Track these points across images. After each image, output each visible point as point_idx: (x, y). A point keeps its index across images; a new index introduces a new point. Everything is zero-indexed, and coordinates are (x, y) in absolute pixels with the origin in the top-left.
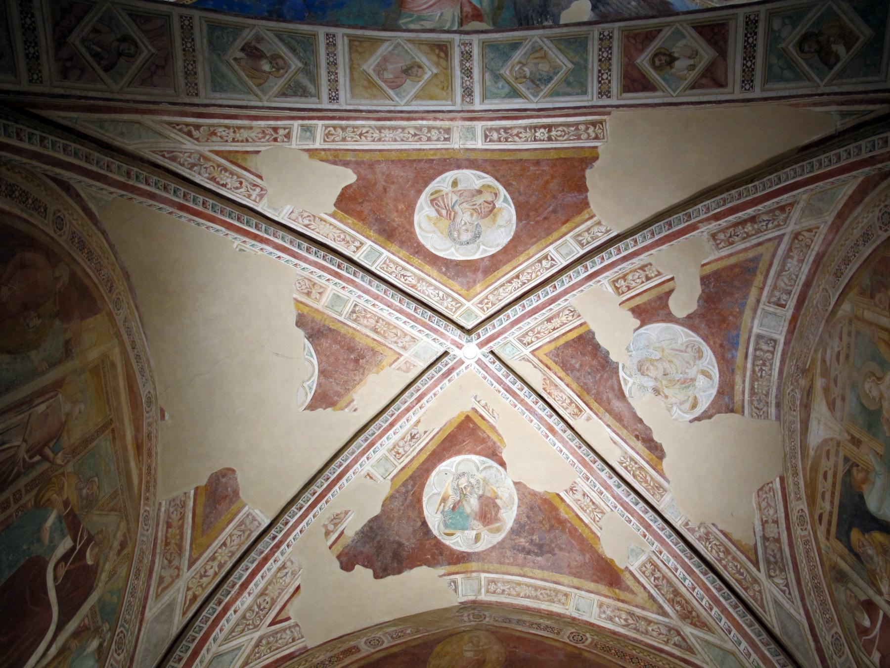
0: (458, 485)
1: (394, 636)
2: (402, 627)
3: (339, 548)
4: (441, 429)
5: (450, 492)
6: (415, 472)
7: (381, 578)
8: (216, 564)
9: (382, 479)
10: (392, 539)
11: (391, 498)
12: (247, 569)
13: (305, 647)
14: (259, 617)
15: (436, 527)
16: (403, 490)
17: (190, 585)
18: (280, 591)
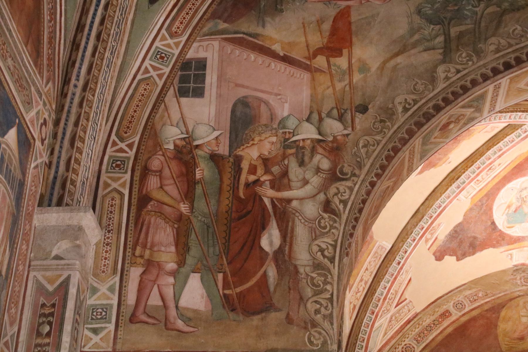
0: (520, 196)
1: (471, 299)
2: (474, 290)
3: (434, 248)
4: (512, 161)
5: (514, 201)
6: (489, 191)
7: (461, 260)
8: (363, 282)
9: (464, 199)
10: (469, 235)
11: (471, 209)
12: (385, 288)
13: (416, 313)
14: (389, 304)
15: (501, 224)
16: (480, 204)
17: (351, 301)
18: (399, 285)
